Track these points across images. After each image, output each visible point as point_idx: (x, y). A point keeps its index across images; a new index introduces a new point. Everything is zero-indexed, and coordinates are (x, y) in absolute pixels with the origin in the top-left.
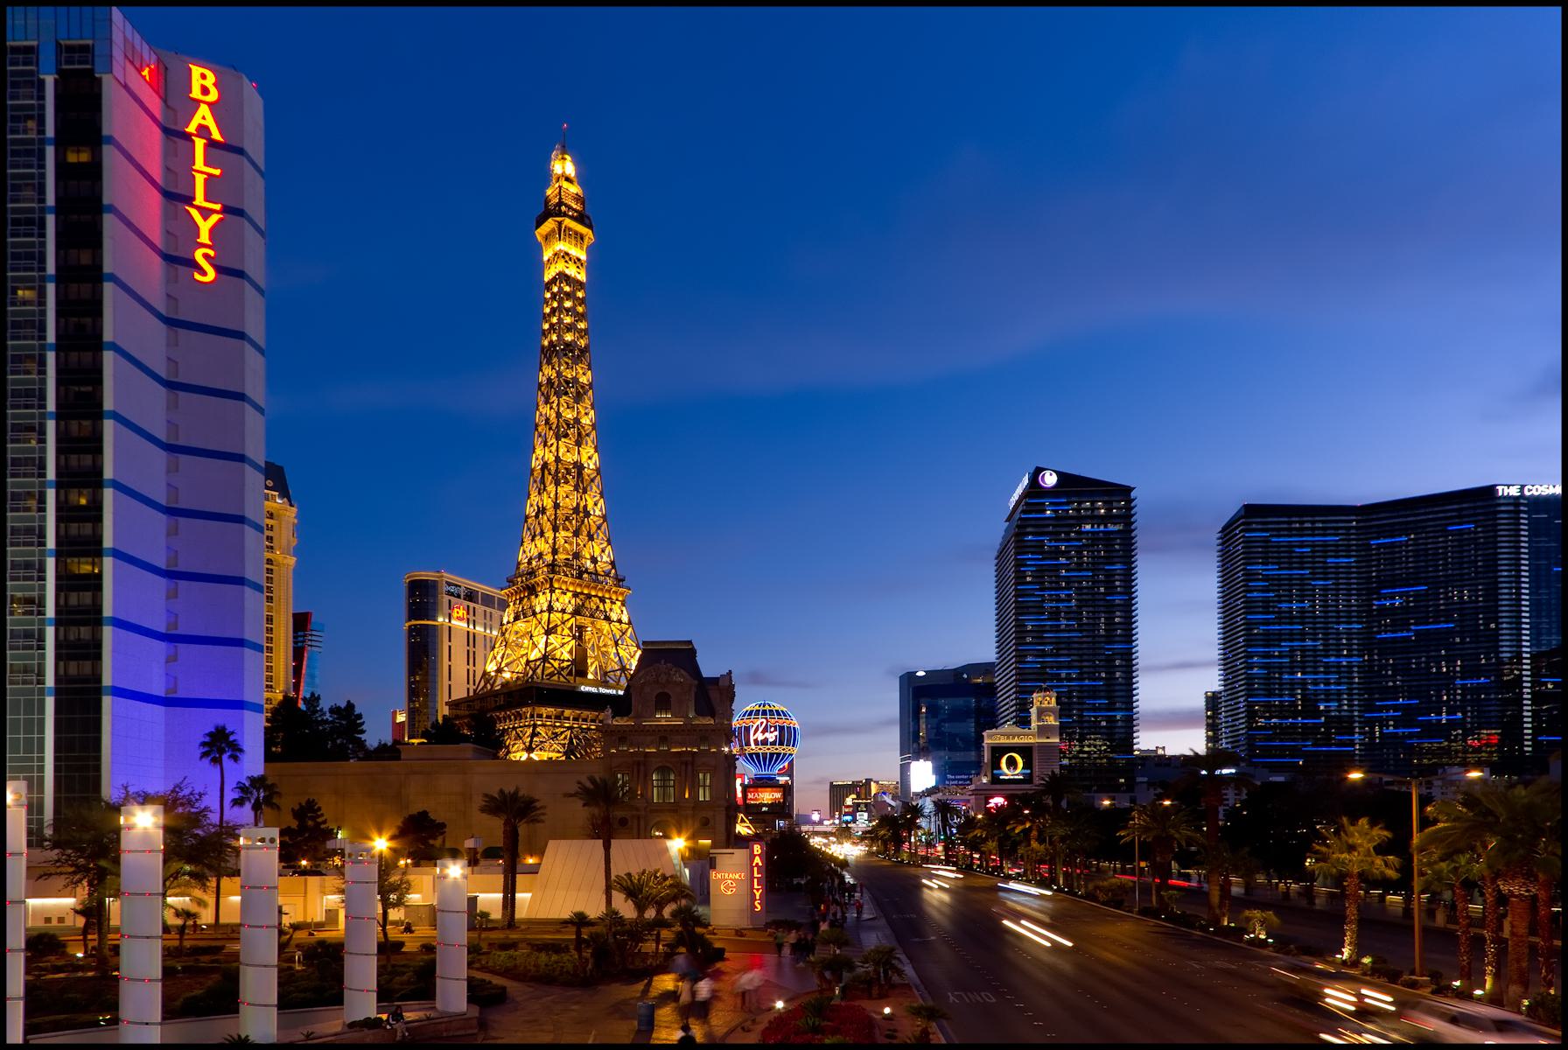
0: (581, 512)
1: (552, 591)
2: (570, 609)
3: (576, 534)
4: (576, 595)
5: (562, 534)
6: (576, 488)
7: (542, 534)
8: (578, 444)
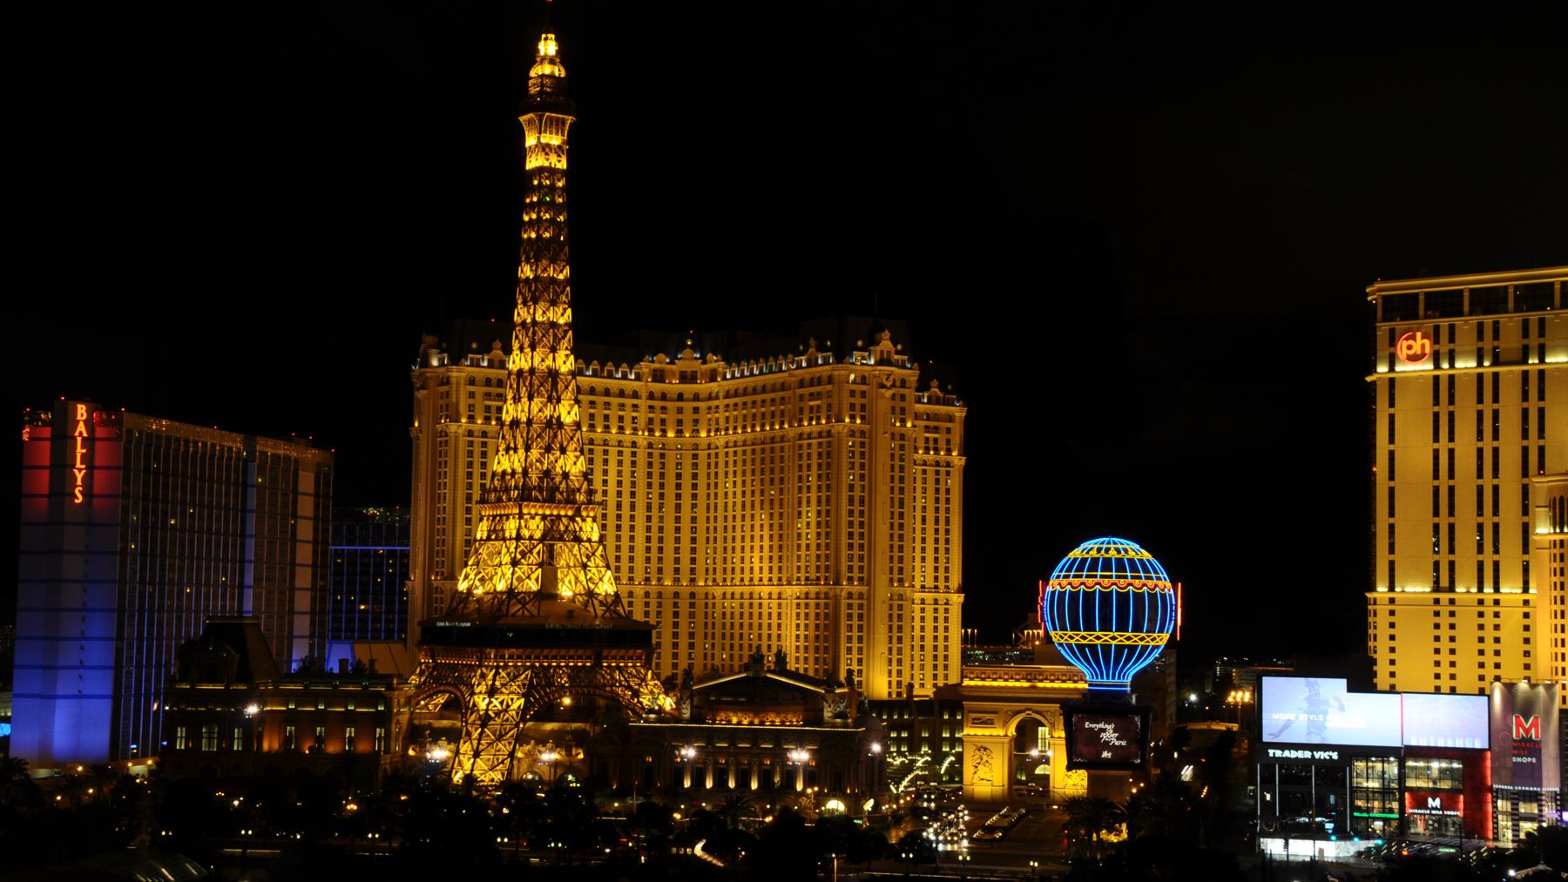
0: (554, 424)
1: (521, 517)
2: (538, 535)
3: (548, 449)
4: (544, 517)
5: (535, 453)
6: (550, 400)
7: (516, 450)
8: (554, 350)
